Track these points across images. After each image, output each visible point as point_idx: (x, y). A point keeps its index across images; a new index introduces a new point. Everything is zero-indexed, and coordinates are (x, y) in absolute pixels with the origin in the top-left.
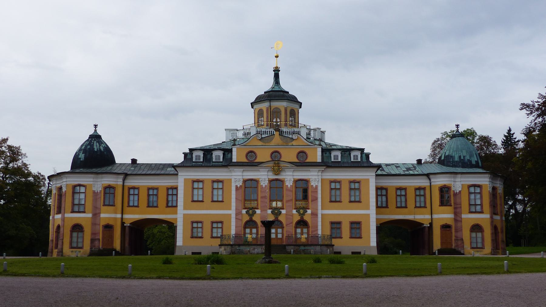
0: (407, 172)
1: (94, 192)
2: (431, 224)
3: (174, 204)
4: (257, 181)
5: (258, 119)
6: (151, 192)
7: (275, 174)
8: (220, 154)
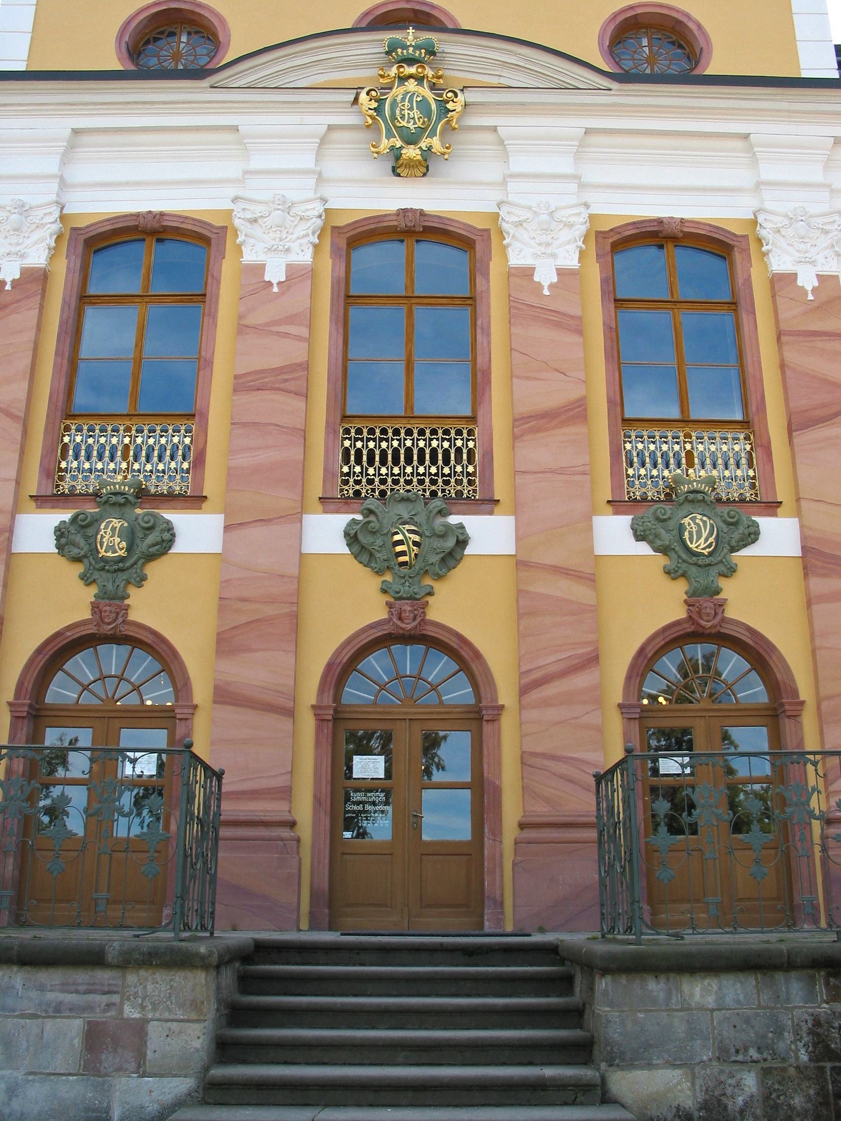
7: (399, 167)
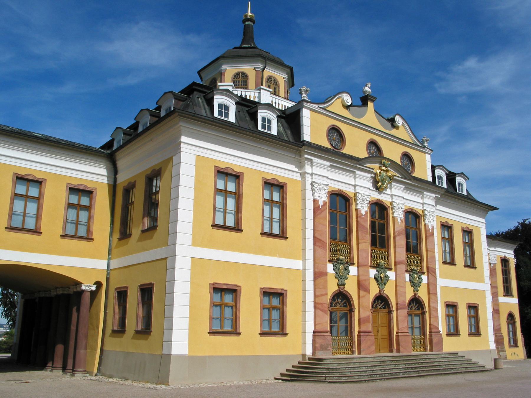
7: (378, 189)
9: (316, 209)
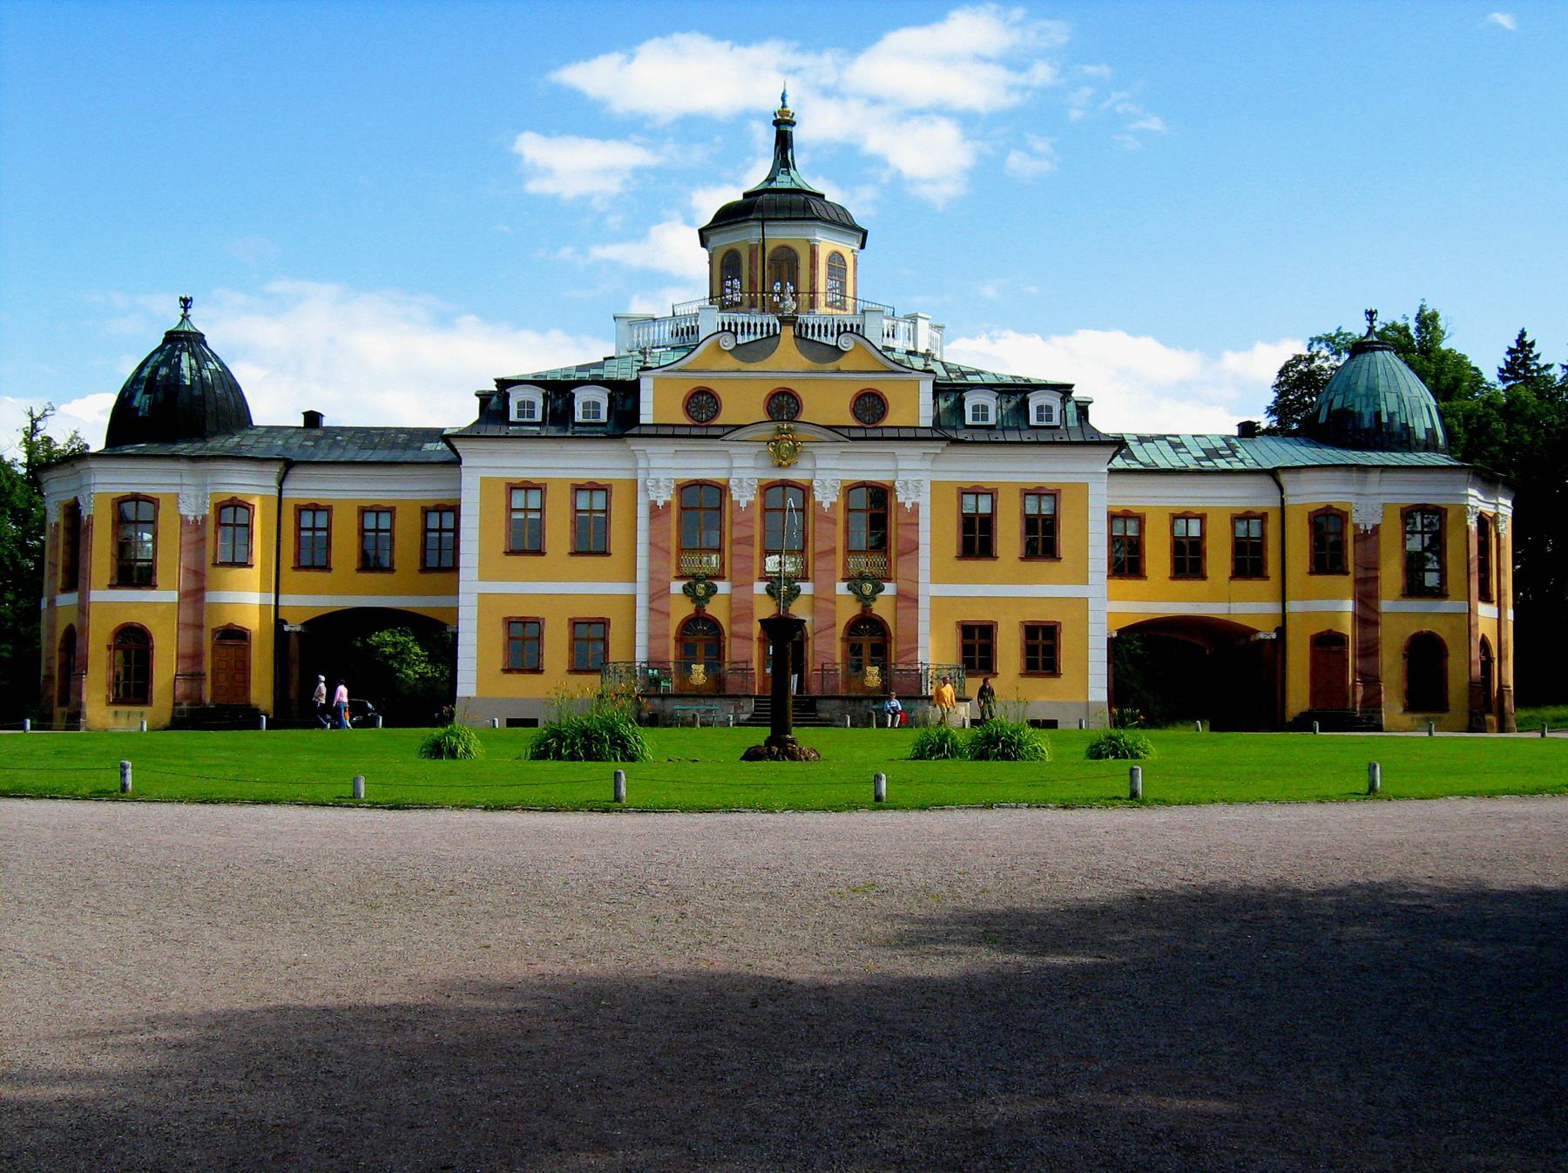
0: (1207, 464)
1: (184, 520)
2: (1281, 631)
3: (447, 562)
4: (721, 489)
5: (723, 281)
6: (370, 522)
8: (601, 396)
9: (654, 510)
